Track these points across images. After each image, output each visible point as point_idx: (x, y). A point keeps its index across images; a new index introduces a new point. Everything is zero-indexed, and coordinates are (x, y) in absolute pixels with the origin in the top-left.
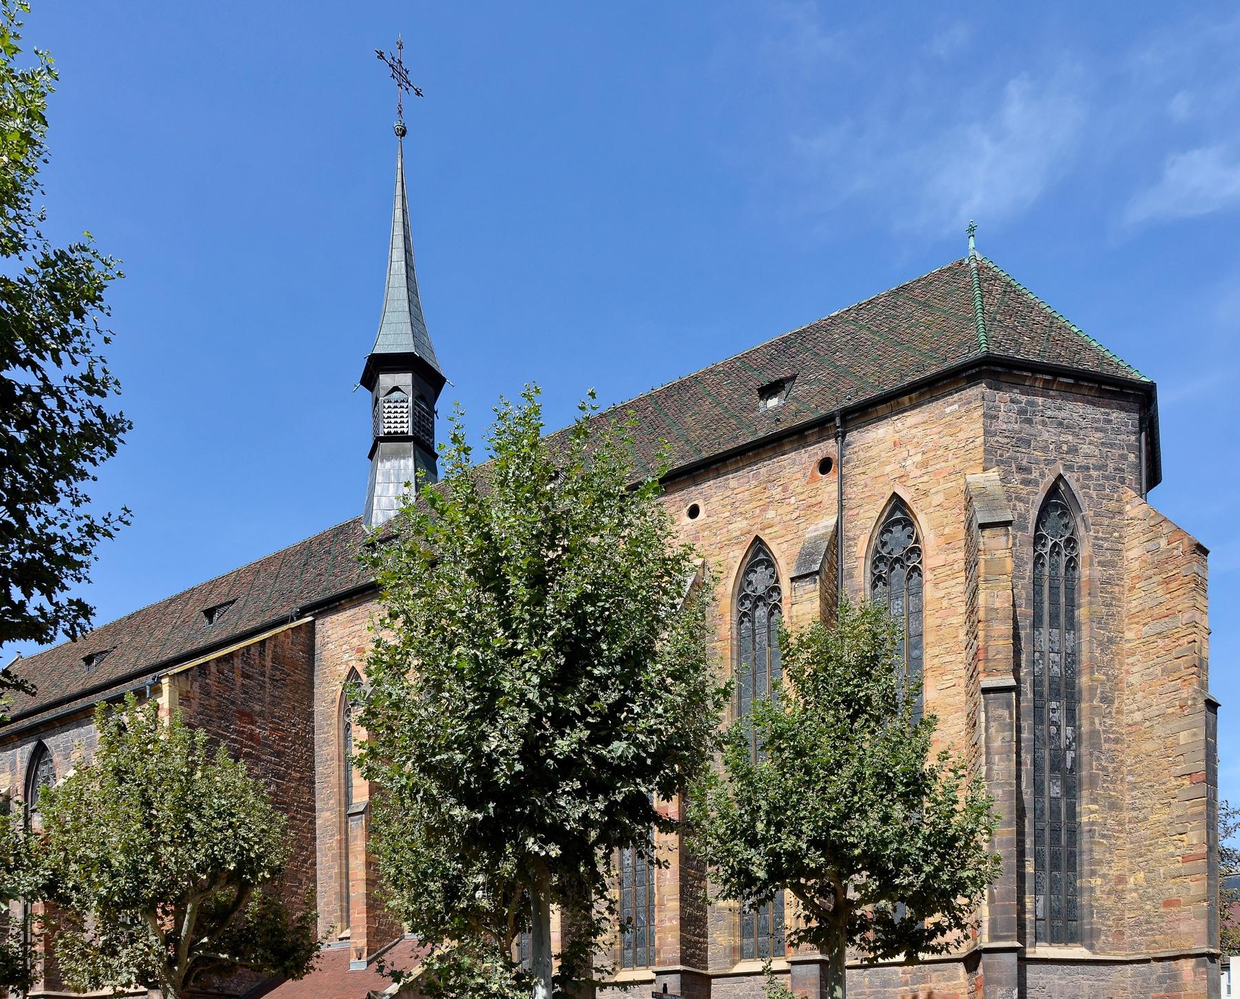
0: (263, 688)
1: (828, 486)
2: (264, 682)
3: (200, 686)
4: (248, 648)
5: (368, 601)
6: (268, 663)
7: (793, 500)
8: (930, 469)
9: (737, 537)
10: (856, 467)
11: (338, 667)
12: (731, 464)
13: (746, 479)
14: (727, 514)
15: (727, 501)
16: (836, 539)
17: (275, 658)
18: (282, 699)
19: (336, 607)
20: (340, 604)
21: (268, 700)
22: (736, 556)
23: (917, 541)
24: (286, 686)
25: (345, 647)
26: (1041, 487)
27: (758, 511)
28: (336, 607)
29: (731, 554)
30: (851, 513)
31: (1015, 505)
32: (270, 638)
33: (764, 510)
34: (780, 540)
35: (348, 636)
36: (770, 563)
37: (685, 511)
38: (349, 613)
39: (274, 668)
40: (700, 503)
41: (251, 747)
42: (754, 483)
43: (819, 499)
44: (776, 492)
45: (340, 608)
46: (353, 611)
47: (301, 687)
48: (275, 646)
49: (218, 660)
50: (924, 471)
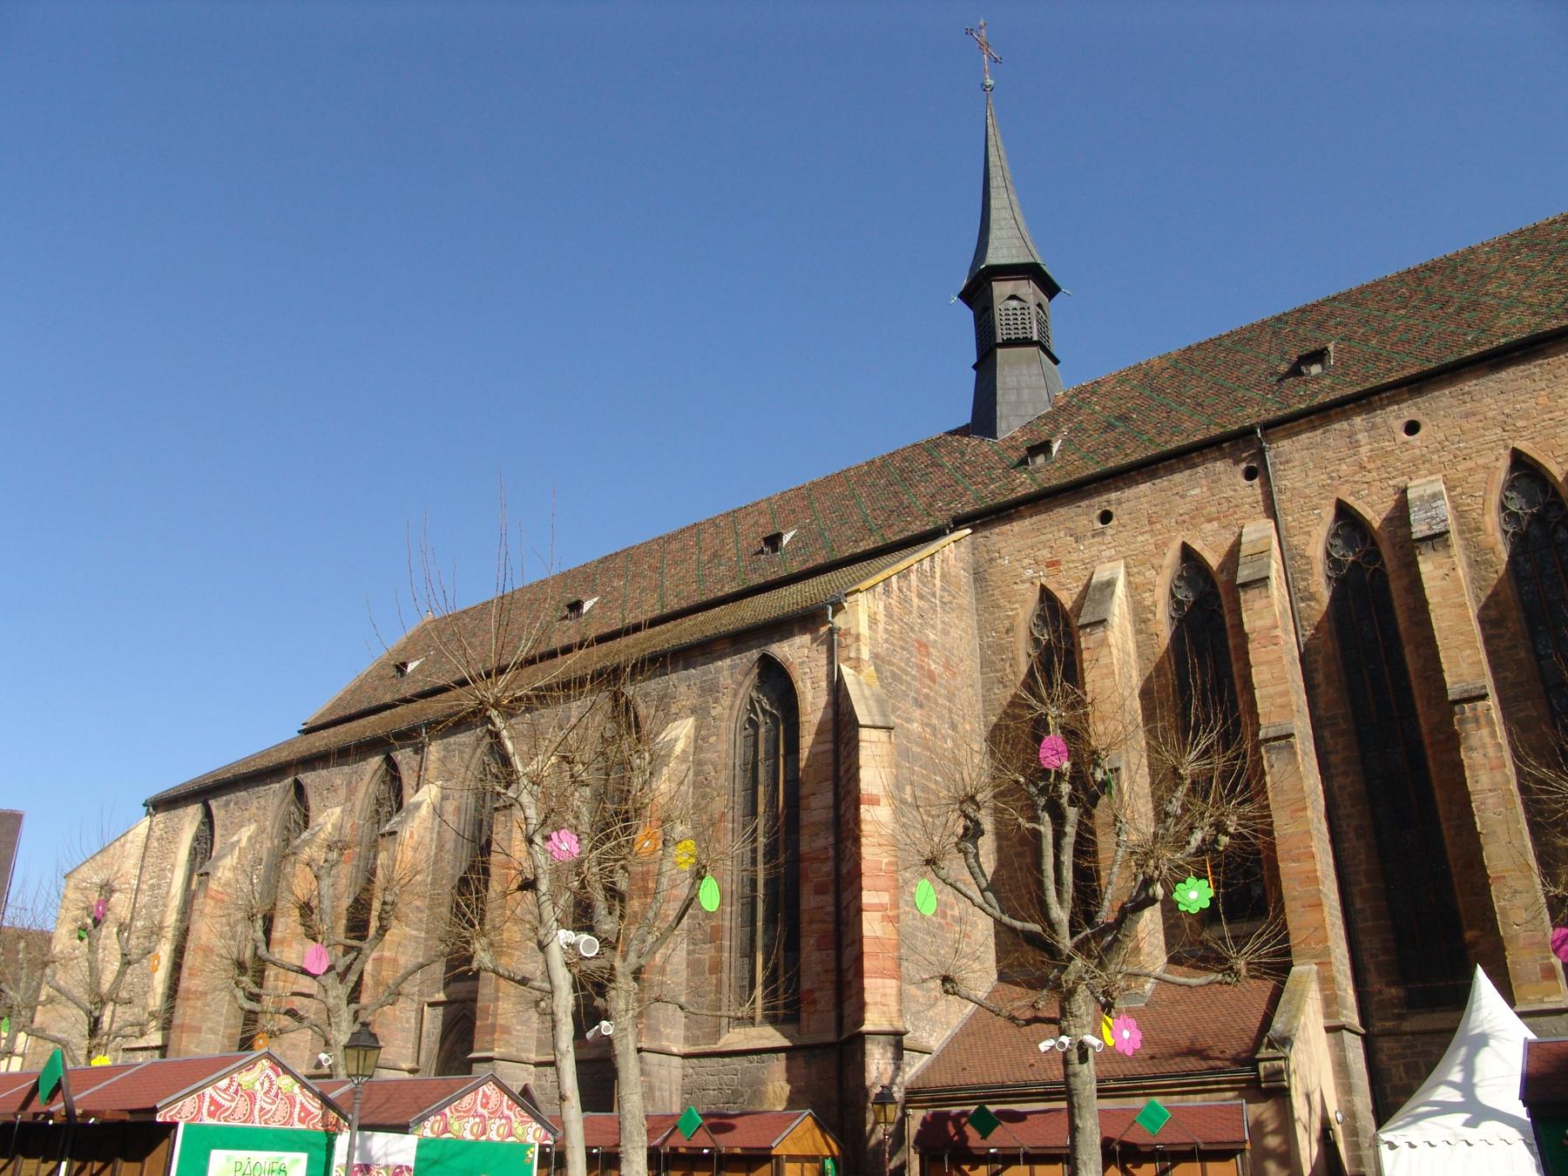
3: (885, 607)
5: (1062, 505)
6: (938, 582)
17: (943, 576)
18: (951, 627)
19: (1011, 514)
20: (1018, 511)
21: (939, 627)
24: (953, 610)
28: (1011, 514)
38: (1027, 522)
39: (943, 589)
41: (930, 688)
46: (1035, 519)
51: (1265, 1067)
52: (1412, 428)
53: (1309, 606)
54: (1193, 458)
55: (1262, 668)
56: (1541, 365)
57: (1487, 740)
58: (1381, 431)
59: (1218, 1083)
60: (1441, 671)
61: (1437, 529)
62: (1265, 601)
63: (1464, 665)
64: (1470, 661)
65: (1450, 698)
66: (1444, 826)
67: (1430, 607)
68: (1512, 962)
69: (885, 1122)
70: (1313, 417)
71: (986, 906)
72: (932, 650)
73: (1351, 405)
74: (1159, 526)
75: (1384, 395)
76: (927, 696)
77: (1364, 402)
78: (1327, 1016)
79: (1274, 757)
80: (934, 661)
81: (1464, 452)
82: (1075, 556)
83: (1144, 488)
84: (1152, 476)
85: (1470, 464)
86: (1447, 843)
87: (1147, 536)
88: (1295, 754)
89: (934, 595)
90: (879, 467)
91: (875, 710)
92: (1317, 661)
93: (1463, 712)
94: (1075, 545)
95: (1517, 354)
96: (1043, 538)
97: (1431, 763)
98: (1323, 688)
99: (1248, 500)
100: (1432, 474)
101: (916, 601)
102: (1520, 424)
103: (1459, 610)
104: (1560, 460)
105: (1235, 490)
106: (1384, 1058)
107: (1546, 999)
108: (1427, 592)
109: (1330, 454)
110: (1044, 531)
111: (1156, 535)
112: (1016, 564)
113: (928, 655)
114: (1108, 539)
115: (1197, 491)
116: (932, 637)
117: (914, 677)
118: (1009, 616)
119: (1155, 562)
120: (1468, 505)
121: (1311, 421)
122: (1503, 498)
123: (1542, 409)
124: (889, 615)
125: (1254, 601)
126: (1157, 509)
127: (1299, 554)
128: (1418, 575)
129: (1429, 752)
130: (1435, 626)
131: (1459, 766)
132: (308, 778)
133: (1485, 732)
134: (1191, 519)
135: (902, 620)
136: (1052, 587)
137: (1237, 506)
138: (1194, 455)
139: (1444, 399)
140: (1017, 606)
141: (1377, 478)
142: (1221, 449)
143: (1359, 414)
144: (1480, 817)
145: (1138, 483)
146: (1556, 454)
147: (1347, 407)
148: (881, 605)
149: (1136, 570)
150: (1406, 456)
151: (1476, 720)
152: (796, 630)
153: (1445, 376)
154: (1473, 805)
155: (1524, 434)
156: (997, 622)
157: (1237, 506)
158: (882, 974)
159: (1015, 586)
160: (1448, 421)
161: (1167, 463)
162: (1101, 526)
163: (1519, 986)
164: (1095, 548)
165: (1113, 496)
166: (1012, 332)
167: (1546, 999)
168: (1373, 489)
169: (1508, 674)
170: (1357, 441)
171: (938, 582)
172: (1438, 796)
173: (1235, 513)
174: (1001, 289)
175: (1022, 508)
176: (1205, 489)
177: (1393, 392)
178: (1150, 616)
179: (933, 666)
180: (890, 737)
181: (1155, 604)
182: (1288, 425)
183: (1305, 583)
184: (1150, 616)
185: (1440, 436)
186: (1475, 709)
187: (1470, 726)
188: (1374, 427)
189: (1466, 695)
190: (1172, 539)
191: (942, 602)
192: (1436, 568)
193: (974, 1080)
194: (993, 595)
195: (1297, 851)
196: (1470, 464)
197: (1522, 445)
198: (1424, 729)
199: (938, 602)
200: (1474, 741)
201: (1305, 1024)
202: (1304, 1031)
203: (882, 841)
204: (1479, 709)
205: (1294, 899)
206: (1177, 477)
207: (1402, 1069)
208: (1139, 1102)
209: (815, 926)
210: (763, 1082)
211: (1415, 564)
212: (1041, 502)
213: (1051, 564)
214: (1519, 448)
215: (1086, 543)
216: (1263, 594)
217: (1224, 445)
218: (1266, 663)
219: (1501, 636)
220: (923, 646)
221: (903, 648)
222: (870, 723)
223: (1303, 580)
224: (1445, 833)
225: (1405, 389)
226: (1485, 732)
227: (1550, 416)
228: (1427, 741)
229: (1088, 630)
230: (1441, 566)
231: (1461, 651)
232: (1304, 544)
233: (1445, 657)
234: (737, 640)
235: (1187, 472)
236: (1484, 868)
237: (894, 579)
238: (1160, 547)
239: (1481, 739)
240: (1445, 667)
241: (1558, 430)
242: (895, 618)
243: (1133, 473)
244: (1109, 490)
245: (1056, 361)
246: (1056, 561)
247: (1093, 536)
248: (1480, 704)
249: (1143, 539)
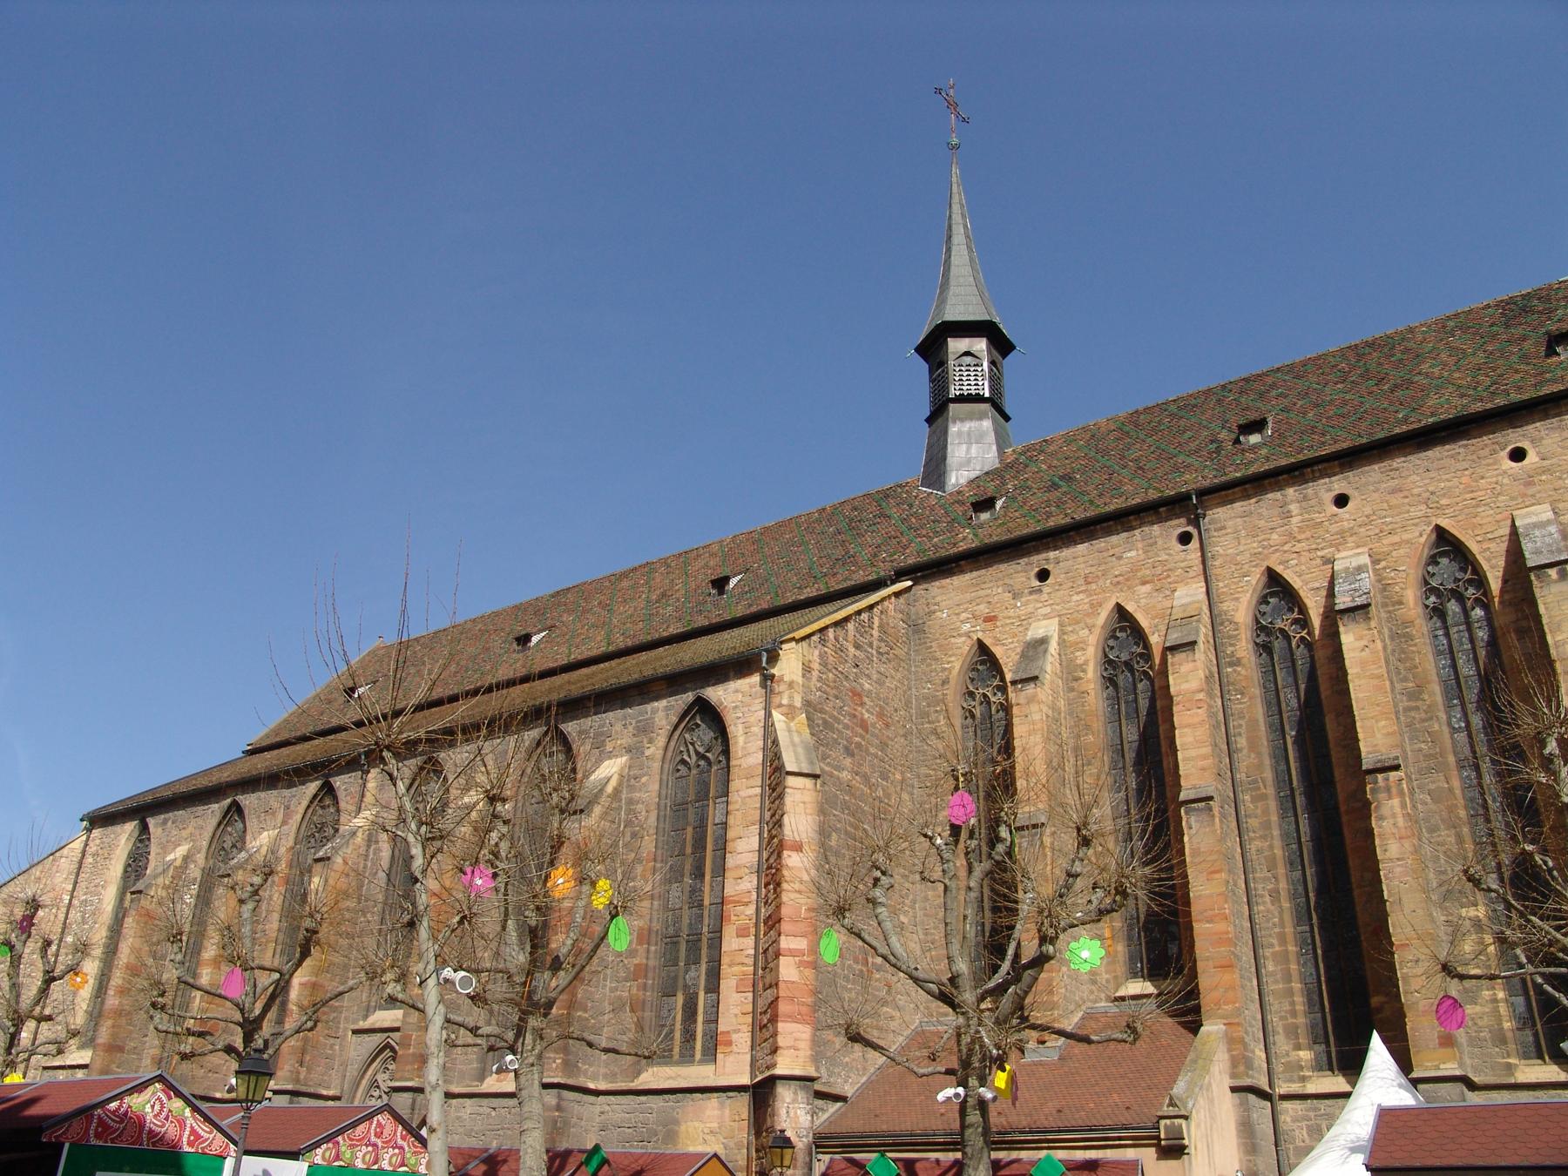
3: (820, 655)
5: (1002, 561)
6: (875, 633)
19: (952, 568)
20: (958, 566)
21: (875, 677)
25: (964, 616)
28: (952, 568)
37: (1505, 454)
38: (968, 576)
39: (881, 640)
40: (1525, 444)
41: (863, 737)
45: (956, 570)
46: (975, 574)
51: (1166, 1124)
52: (1341, 501)
53: (1235, 671)
54: (1130, 521)
55: (1186, 730)
56: (1466, 446)
57: (1398, 810)
58: (1312, 502)
59: (1120, 1138)
60: (1358, 740)
61: (1359, 601)
62: (1191, 665)
63: (1379, 736)
64: (1384, 731)
65: (1364, 768)
66: (1356, 893)
67: (1349, 677)
68: (1412, 1029)
69: (782, 1166)
70: (1247, 486)
71: (892, 958)
73: (1285, 476)
74: (1094, 586)
75: (1316, 468)
76: (859, 745)
77: (1297, 473)
78: (1233, 1076)
79: (1193, 819)
80: (867, 711)
81: (1390, 527)
82: (1011, 613)
83: (1082, 548)
84: (1091, 537)
85: (1396, 539)
86: (1358, 908)
87: (1081, 596)
88: (1213, 816)
89: (871, 645)
90: (827, 515)
91: (802, 757)
92: (1240, 726)
93: (1376, 782)
94: (1012, 602)
95: (1443, 434)
96: (982, 593)
97: (1346, 832)
98: (1245, 752)
99: (1183, 565)
100: (1358, 547)
101: (852, 650)
102: (1444, 502)
103: (1376, 682)
104: (1479, 538)
105: (1169, 554)
106: (1288, 1119)
107: (1442, 1066)
108: (1347, 663)
109: (1262, 523)
110: (983, 586)
111: (1091, 595)
112: (955, 618)
113: (862, 704)
114: (1045, 596)
115: (1133, 553)
116: (867, 686)
117: (847, 727)
118: (944, 669)
119: (1089, 621)
120: (1392, 578)
121: (1245, 489)
122: (1257, 613)
123: (1464, 489)
124: (824, 664)
125: (1180, 664)
126: (1093, 569)
127: (1228, 620)
128: (1340, 644)
129: (1345, 819)
130: (1353, 696)
131: (1370, 834)
132: (248, 800)
133: (1396, 802)
134: (1125, 582)
135: (837, 669)
136: (988, 642)
137: (1169, 570)
138: (1131, 518)
139: (1372, 474)
140: (953, 659)
141: (1307, 548)
142: (1157, 513)
143: (1293, 485)
144: (1388, 885)
145: (1076, 543)
146: (1477, 532)
147: (1280, 478)
148: (817, 652)
149: (1070, 629)
150: (1334, 528)
151: (1388, 789)
152: (732, 674)
153: (1375, 452)
154: (1382, 873)
155: (1447, 511)
156: (933, 674)
157: (1169, 570)
158: (792, 1018)
159: (953, 640)
160: (1375, 495)
161: (1105, 525)
162: (1038, 583)
163: (1418, 1052)
164: (1032, 606)
165: (1052, 554)
166: (964, 388)
167: (1442, 1066)
168: (1303, 559)
169: (1423, 746)
170: (1288, 512)
171: (875, 633)
172: (1351, 863)
173: (1169, 576)
174: (956, 345)
175: (962, 563)
176: (1140, 552)
177: (1326, 465)
178: (1082, 674)
179: (866, 715)
180: (816, 784)
181: (1086, 662)
182: (1223, 493)
183: (1231, 649)
184: (1082, 674)
185: (1368, 510)
186: (1387, 779)
187: (1382, 796)
188: (1305, 498)
189: (1379, 765)
190: (1106, 599)
192: (1356, 640)
193: (884, 1127)
194: (931, 647)
195: (1211, 913)
196: (1396, 539)
197: (1445, 523)
198: (1341, 797)
200: (1385, 811)
201: (1210, 1084)
202: (1208, 1090)
203: (803, 888)
204: (1391, 779)
205: (1208, 959)
206: (1114, 539)
207: (1305, 1132)
208: (1043, 1154)
209: (736, 969)
210: (677, 1122)
211: (1337, 634)
212: (981, 558)
213: (990, 619)
214: (1442, 525)
215: (1023, 599)
216: (1190, 659)
217: (1161, 509)
218: (1188, 726)
219: (1417, 708)
220: (857, 695)
221: (837, 697)
222: (796, 770)
223: (1231, 645)
224: (1356, 900)
225: (1336, 462)
226: (1396, 802)
227: (1472, 495)
228: (1343, 808)
229: (1020, 686)
230: (1361, 638)
231: (1377, 721)
232: (1233, 610)
233: (1362, 727)
234: (673, 682)
235: (1125, 535)
236: (1389, 936)
238: (1095, 607)
239: (1392, 807)
240: (1360, 736)
241: (1480, 510)
242: (830, 667)
243: (1071, 533)
244: (1048, 548)
245: (1007, 418)
246: (994, 616)
247: (1031, 593)
248: (1393, 775)
249: (1078, 598)
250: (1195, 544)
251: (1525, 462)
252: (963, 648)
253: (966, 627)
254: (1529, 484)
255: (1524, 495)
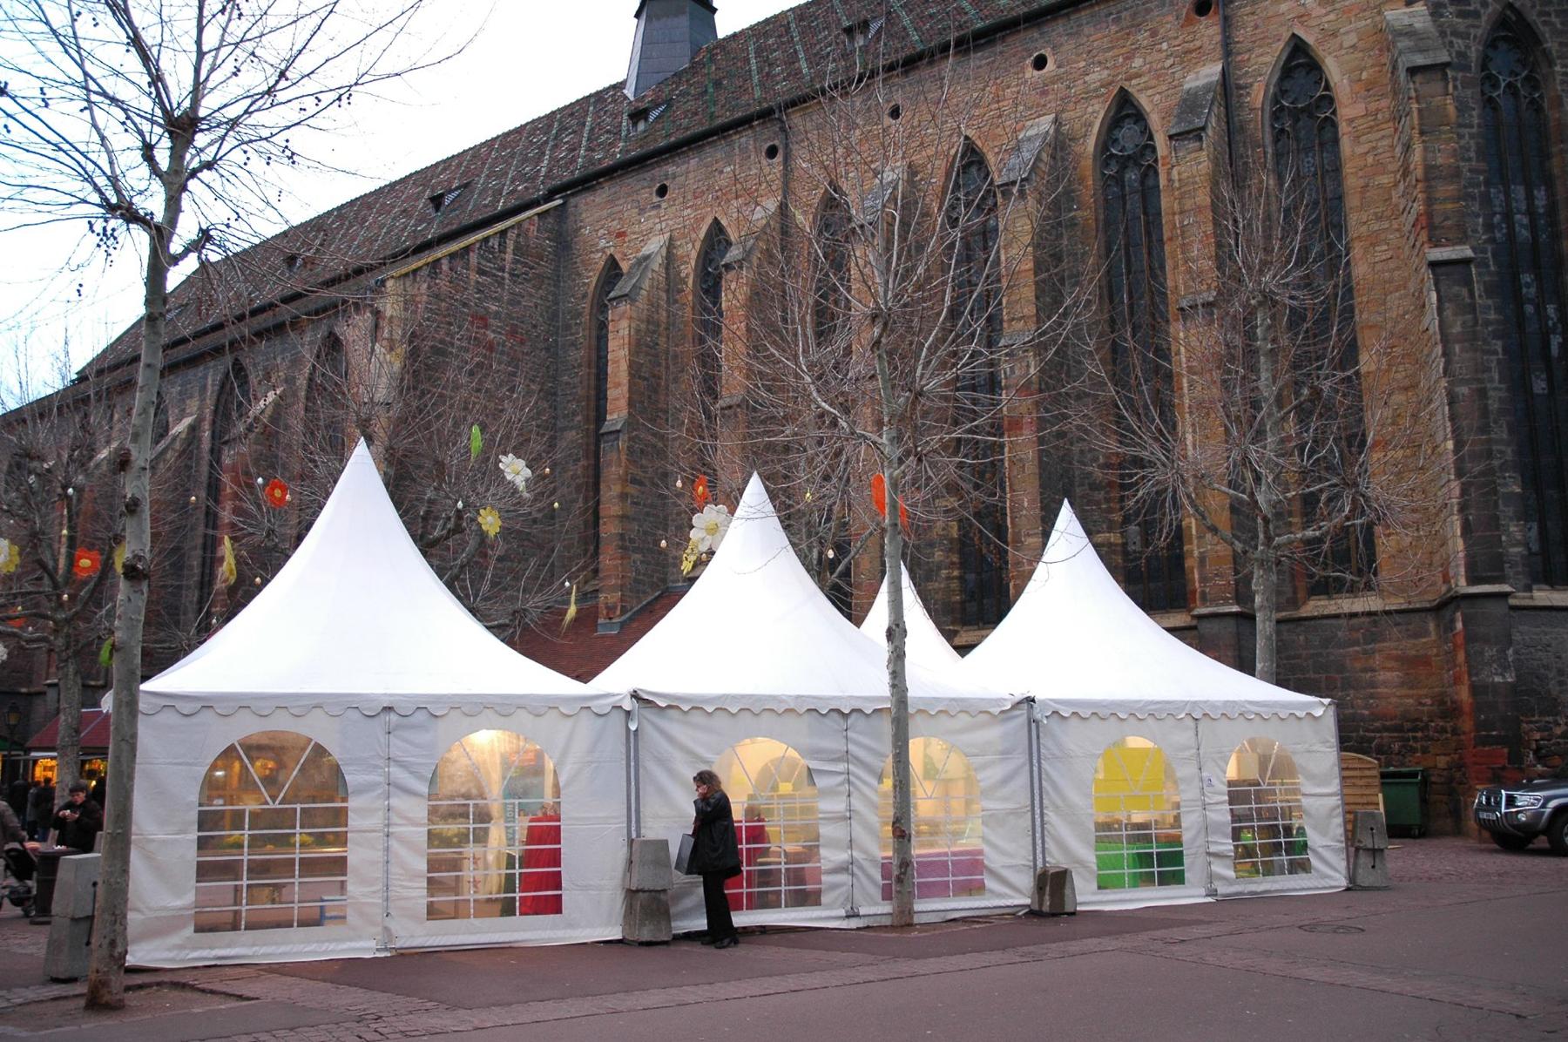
0: (501, 285)
1: (1209, 29)
2: (503, 278)
4: (486, 240)
6: (509, 256)
7: (1165, 46)
8: (1337, 6)
9: (1096, 90)
10: (1240, 7)
11: (592, 256)
12: (1084, 8)
13: (1104, 25)
14: (1082, 64)
15: (1081, 49)
16: (1228, 88)
17: (518, 249)
22: (1097, 112)
23: (1327, 88)
25: (602, 231)
26: (1484, 18)
27: (1121, 60)
29: (1090, 109)
30: (1239, 58)
31: (1451, 42)
32: (512, 227)
33: (1129, 57)
34: (1150, 92)
35: (606, 219)
36: (1139, 117)
37: (1029, 61)
39: (516, 262)
40: (1047, 52)
42: (1114, 28)
43: (1198, 43)
44: (1143, 37)
47: (546, 281)
48: (518, 235)
49: (452, 256)
50: (1329, 9)
54: (730, 135)
72: (492, 321)
80: (493, 331)
82: (636, 227)
89: (502, 269)
95: (982, 41)
101: (474, 277)
104: (996, 150)
113: (486, 326)
118: (585, 284)
134: (722, 198)
136: (618, 257)
142: (752, 127)
146: (996, 143)
162: (656, 199)
165: (671, 169)
171: (509, 256)
191: (512, 275)
199: (506, 275)
213: (621, 235)
220: (482, 320)
237: (445, 262)
250: (779, 158)
251: (1045, 70)
252: (599, 260)
253: (603, 243)
254: (1044, 93)
255: (1038, 105)
